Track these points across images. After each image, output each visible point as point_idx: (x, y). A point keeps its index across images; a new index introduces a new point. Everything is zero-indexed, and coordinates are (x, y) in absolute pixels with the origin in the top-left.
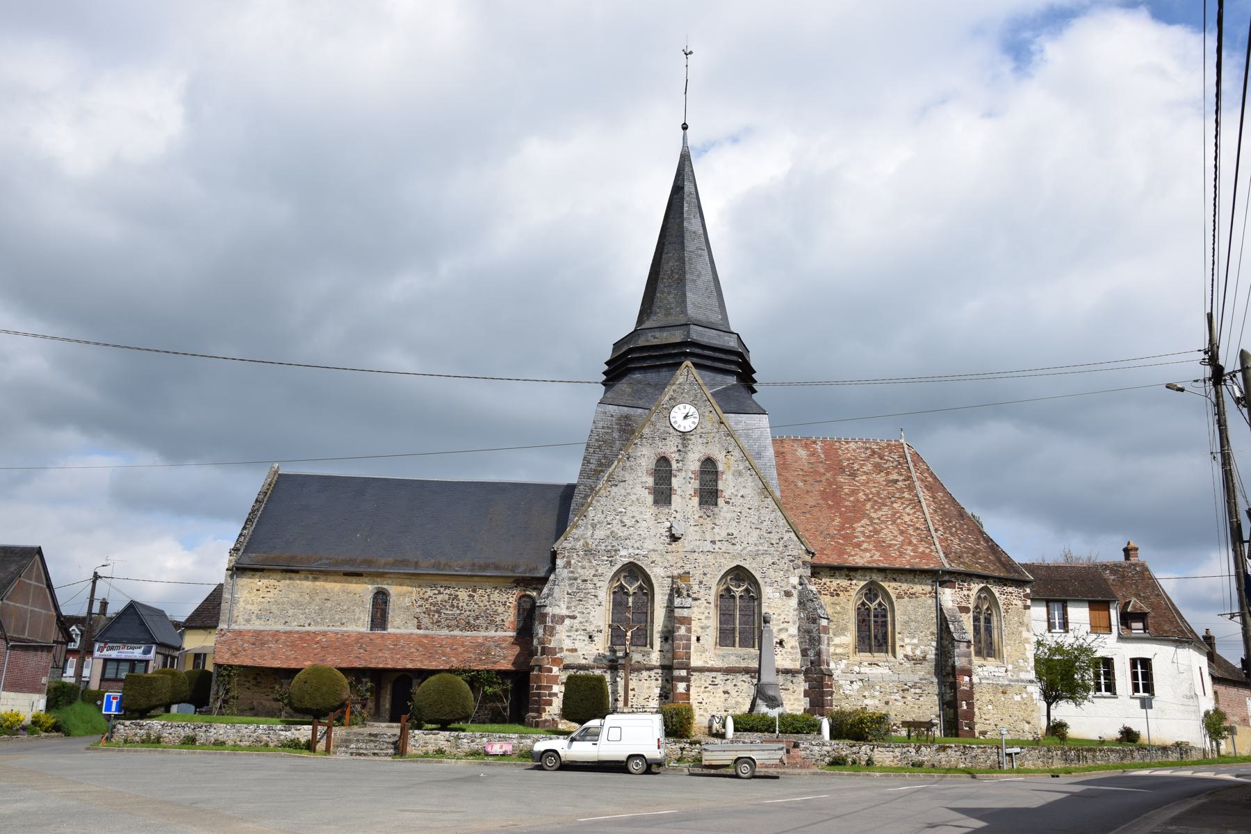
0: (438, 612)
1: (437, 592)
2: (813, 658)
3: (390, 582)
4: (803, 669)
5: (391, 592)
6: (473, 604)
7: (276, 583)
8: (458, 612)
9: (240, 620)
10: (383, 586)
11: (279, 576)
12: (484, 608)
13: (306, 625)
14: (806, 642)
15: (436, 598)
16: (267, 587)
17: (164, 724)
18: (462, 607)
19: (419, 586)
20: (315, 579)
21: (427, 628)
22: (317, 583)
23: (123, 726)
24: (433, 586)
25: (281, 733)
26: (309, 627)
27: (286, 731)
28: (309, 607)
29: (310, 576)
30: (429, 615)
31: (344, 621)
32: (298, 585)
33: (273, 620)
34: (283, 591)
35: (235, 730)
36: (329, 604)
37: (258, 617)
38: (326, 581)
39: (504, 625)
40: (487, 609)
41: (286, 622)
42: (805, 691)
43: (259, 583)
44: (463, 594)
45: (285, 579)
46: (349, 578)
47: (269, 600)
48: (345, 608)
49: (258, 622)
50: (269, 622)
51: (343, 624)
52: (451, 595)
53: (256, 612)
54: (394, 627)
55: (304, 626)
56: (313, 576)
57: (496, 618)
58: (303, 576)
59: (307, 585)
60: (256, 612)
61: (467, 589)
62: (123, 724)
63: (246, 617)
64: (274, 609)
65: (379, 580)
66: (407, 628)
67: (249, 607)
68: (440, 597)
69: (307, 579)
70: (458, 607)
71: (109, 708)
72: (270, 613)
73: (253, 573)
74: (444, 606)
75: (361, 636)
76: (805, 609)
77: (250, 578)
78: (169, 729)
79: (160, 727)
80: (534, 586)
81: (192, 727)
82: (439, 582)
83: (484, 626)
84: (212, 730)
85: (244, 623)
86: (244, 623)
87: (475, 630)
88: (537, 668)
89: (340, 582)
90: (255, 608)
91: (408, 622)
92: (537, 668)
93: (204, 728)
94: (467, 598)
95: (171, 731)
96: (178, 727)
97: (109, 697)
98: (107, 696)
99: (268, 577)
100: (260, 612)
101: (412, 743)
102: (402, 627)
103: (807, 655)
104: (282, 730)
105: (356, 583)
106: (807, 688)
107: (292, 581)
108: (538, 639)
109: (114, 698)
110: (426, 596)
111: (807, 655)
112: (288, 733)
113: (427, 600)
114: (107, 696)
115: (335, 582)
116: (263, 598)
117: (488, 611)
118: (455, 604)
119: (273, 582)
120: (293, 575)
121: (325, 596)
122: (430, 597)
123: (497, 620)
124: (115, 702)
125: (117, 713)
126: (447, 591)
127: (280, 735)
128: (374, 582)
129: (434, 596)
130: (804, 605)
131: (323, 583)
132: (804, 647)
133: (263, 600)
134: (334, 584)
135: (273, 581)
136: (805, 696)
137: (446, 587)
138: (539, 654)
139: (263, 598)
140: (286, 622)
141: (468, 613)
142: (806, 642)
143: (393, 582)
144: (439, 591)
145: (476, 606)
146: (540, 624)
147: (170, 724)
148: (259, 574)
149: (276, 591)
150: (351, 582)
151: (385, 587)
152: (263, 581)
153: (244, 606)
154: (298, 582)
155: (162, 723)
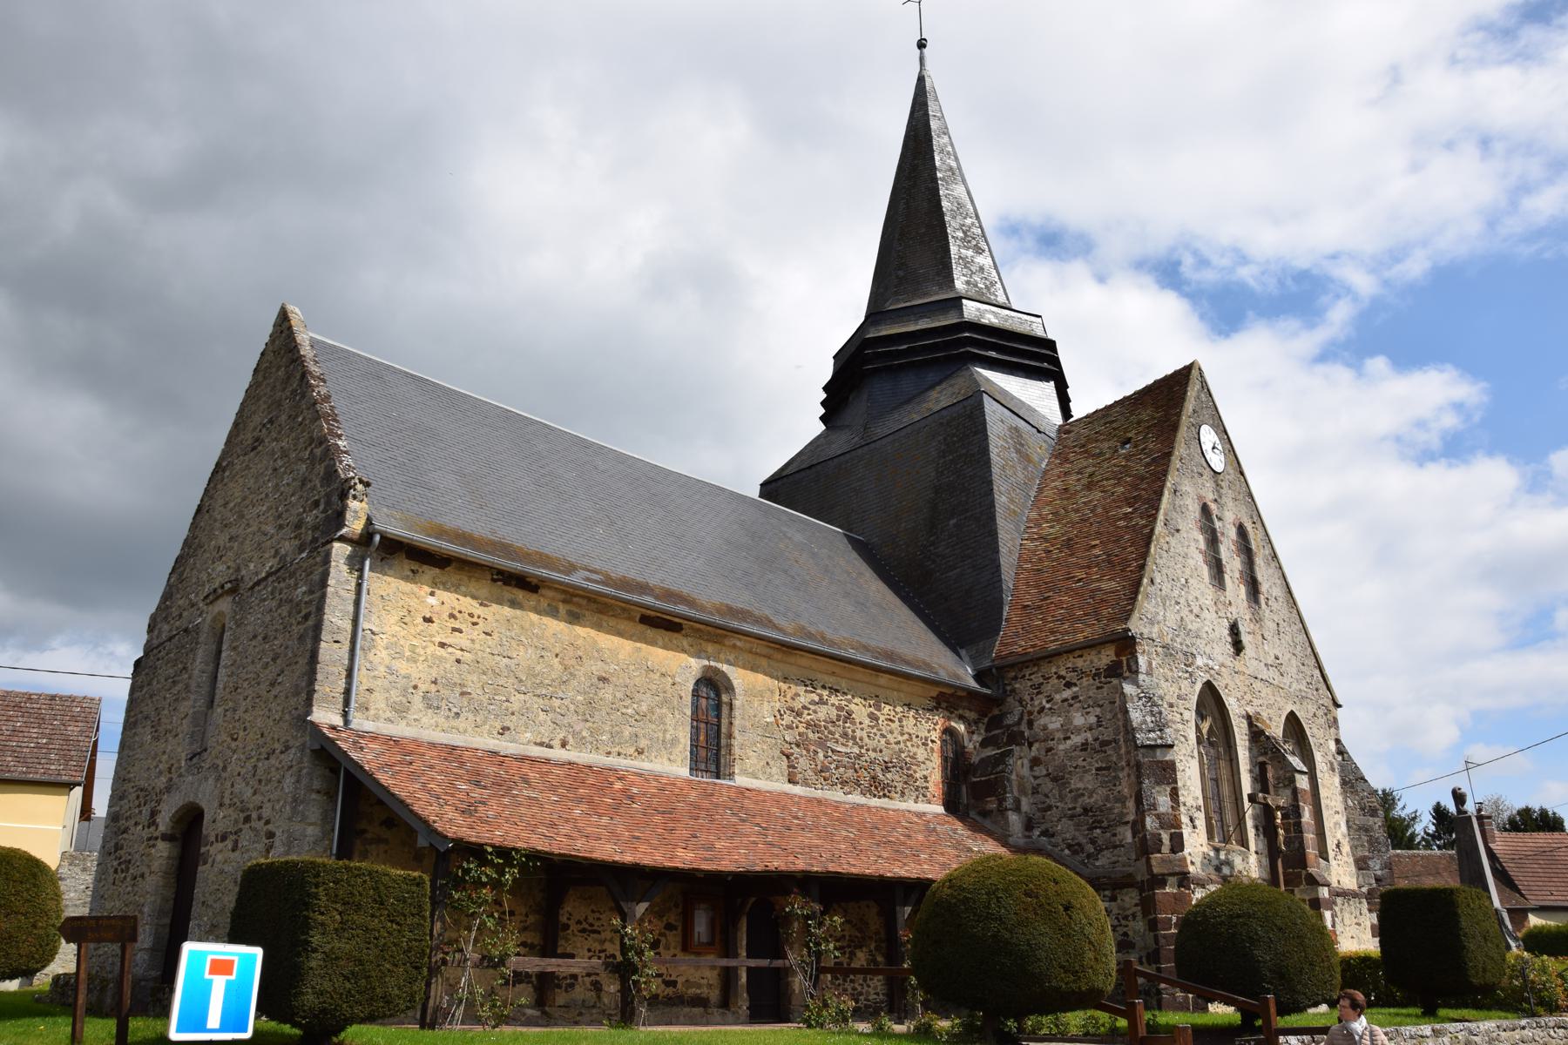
0: (822, 743)
1: (817, 699)
2: (1379, 873)
3: (731, 658)
4: (1364, 890)
5: (735, 683)
6: (877, 738)
7: (478, 610)
8: (856, 750)
9: (378, 702)
10: (719, 665)
11: (484, 588)
12: (897, 747)
13: (556, 743)
14: (1362, 846)
15: (815, 712)
16: (452, 616)
18: (861, 739)
19: (785, 679)
20: (574, 618)
21: (806, 783)
22: (581, 631)
24: (810, 683)
26: (563, 751)
28: (561, 694)
29: (562, 608)
30: (808, 751)
31: (643, 743)
32: (532, 624)
33: (471, 716)
34: (495, 635)
36: (607, 693)
37: (430, 704)
38: (598, 627)
42: (1373, 926)
43: (431, 600)
44: (860, 710)
45: (500, 602)
46: (650, 632)
48: (644, 708)
49: (428, 718)
50: (460, 723)
51: (640, 752)
52: (840, 708)
53: (423, 687)
54: (744, 772)
56: (568, 607)
57: (915, 772)
58: (544, 604)
59: (555, 628)
60: (423, 687)
61: (865, 699)
63: (395, 695)
64: (473, 683)
65: (710, 648)
66: (770, 777)
67: (402, 666)
68: (823, 713)
69: (553, 613)
70: (854, 738)
72: (463, 694)
73: (415, 566)
74: (830, 732)
75: (666, 785)
76: (1355, 792)
77: (406, 579)
80: (961, 712)
82: (819, 676)
83: (900, 786)
85: (388, 714)
87: (885, 795)
88: (1172, 880)
89: (630, 638)
90: (420, 673)
91: (771, 763)
92: (1172, 880)
94: (867, 721)
99: (455, 588)
100: (433, 688)
103: (1368, 868)
105: (665, 647)
107: (518, 612)
108: (1158, 816)
110: (797, 705)
111: (1368, 868)
113: (799, 714)
115: (620, 634)
116: (442, 645)
117: (903, 755)
119: (468, 604)
120: (520, 595)
121: (597, 668)
122: (805, 707)
123: (918, 775)
126: (833, 700)
129: (812, 707)
130: (1352, 787)
131: (593, 633)
133: (441, 652)
134: (616, 640)
135: (469, 599)
137: (834, 691)
138: (1166, 848)
139: (442, 645)
141: (873, 755)
142: (1362, 846)
144: (820, 696)
145: (883, 741)
146: (1158, 783)
149: (476, 633)
150: (653, 643)
151: (725, 668)
152: (442, 594)
153: (387, 660)
154: (534, 617)
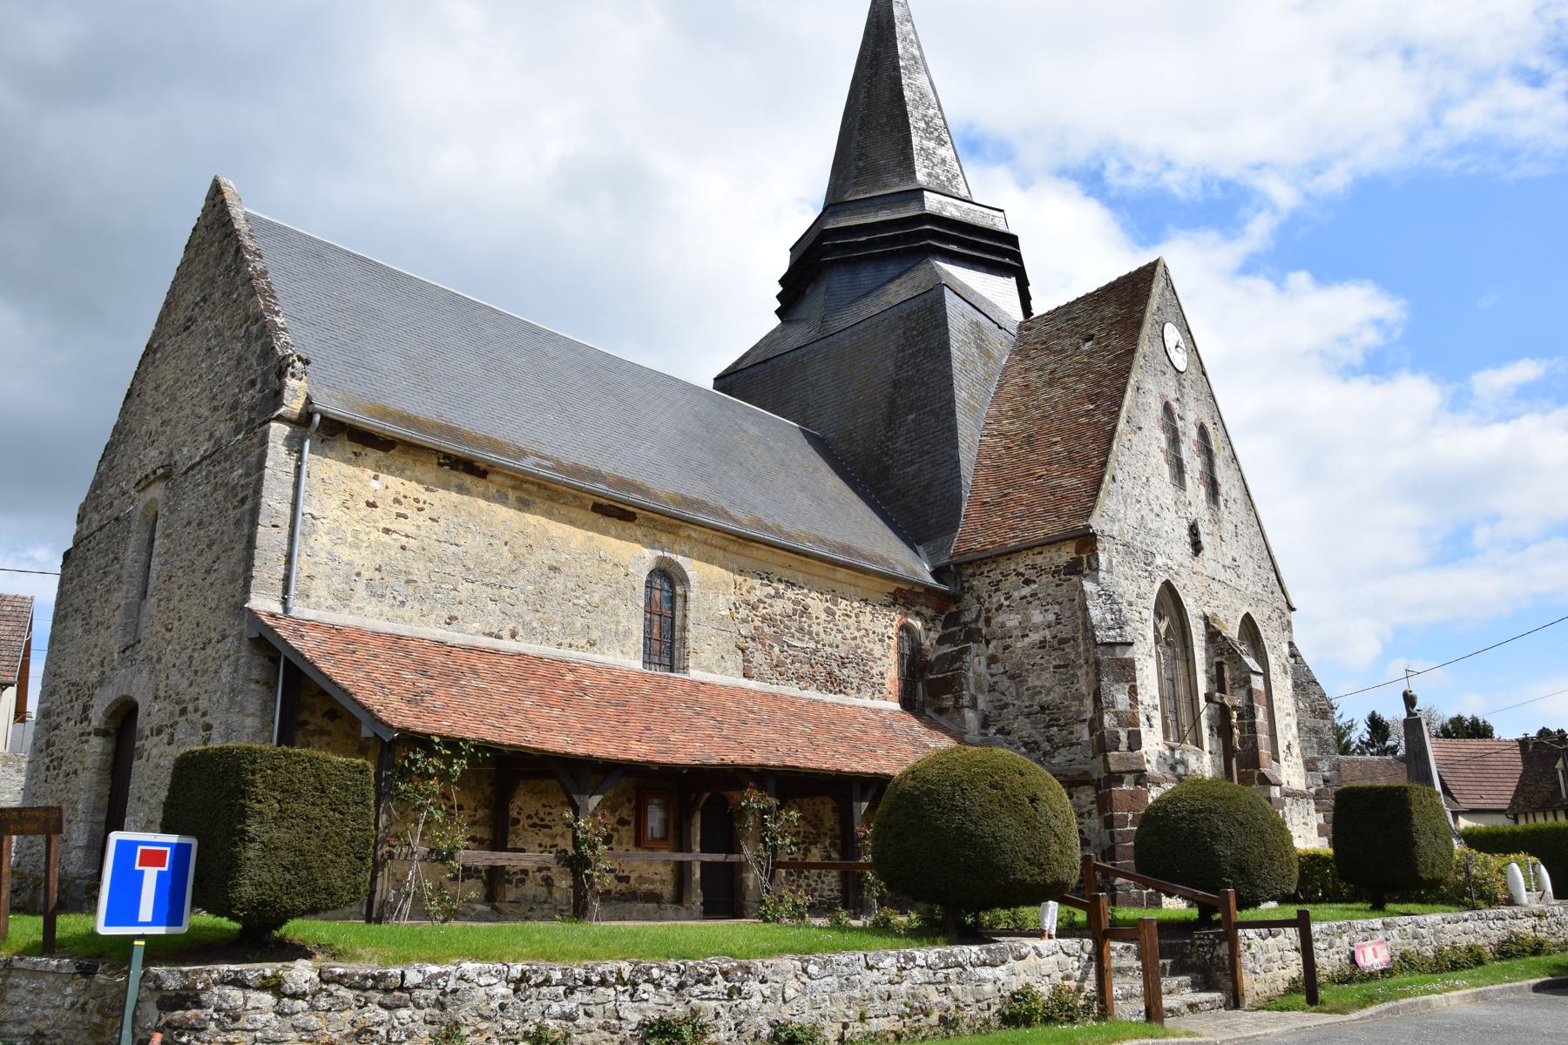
0: (777, 637)
1: (773, 592)
2: (1327, 774)
3: (686, 549)
4: (1312, 790)
5: (690, 574)
6: (834, 633)
7: (425, 496)
8: (812, 645)
9: (320, 589)
10: (673, 556)
11: (431, 472)
12: (853, 643)
13: (506, 633)
14: (1312, 747)
15: (771, 606)
16: (396, 501)
17: (524, 978)
18: (817, 635)
19: (741, 572)
20: (524, 505)
21: (761, 678)
22: (531, 518)
23: (267, 999)
24: (766, 577)
25: (986, 972)
26: (512, 642)
27: (993, 965)
28: (510, 584)
29: (512, 495)
30: (764, 645)
31: (595, 635)
32: (481, 511)
33: (416, 605)
34: (442, 522)
35: (833, 981)
36: (558, 582)
37: (374, 593)
38: (549, 514)
39: (883, 684)
40: (858, 647)
41: (453, 618)
42: (1319, 827)
43: (375, 484)
44: (817, 604)
45: (446, 487)
46: (603, 521)
47: (404, 540)
48: (596, 599)
49: (372, 607)
50: (406, 612)
51: (592, 644)
52: (796, 602)
53: (366, 575)
54: (699, 666)
55: (499, 637)
56: (518, 494)
57: (872, 668)
58: (493, 490)
59: (504, 515)
60: (366, 575)
61: (822, 594)
62: (274, 986)
63: (337, 583)
64: (419, 570)
65: (664, 538)
66: (724, 671)
67: (344, 553)
68: (779, 607)
69: (502, 499)
70: (810, 633)
71: (124, 909)
72: (408, 582)
73: (357, 448)
74: (786, 627)
75: (619, 678)
76: (1307, 695)
77: (348, 461)
78: (556, 998)
79: (502, 990)
80: (918, 608)
81: (673, 980)
82: (776, 569)
83: (856, 682)
84: (753, 985)
85: (330, 602)
86: (330, 602)
87: (840, 691)
88: (1129, 778)
89: (582, 526)
90: (362, 559)
91: (726, 657)
92: (1129, 778)
93: (720, 984)
94: (823, 616)
95: (569, 1005)
96: (603, 982)
97: (126, 848)
98: (120, 843)
99: (401, 473)
100: (377, 575)
101: (1250, 965)
102: (714, 668)
103: (1316, 770)
104: (984, 964)
105: (618, 537)
106: (1322, 821)
107: (466, 498)
108: (1116, 714)
109: (152, 858)
110: (753, 599)
111: (1316, 770)
112: (1000, 972)
113: (754, 608)
114: (120, 843)
115: (571, 522)
116: (387, 531)
117: (859, 651)
118: (806, 627)
119: (413, 488)
120: (468, 480)
121: (548, 557)
122: (760, 601)
123: (874, 672)
124: (151, 875)
125: (161, 930)
126: (790, 594)
127: (981, 981)
128: (655, 541)
129: (768, 601)
130: (1304, 689)
131: (544, 520)
132: (1309, 755)
133: (385, 538)
134: (568, 528)
135: (414, 484)
136: (1319, 836)
137: (791, 584)
138: (1123, 746)
139: (387, 531)
140: (453, 618)
141: (829, 650)
142: (1312, 747)
143: (691, 549)
144: (776, 589)
145: (839, 636)
146: (1117, 681)
147: (557, 975)
148: (374, 455)
149: (422, 519)
150: (605, 532)
151: (679, 559)
152: (386, 478)
153: (329, 546)
154: (482, 503)
155: (516, 970)
